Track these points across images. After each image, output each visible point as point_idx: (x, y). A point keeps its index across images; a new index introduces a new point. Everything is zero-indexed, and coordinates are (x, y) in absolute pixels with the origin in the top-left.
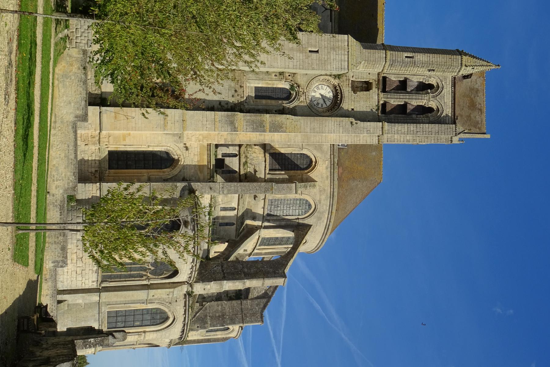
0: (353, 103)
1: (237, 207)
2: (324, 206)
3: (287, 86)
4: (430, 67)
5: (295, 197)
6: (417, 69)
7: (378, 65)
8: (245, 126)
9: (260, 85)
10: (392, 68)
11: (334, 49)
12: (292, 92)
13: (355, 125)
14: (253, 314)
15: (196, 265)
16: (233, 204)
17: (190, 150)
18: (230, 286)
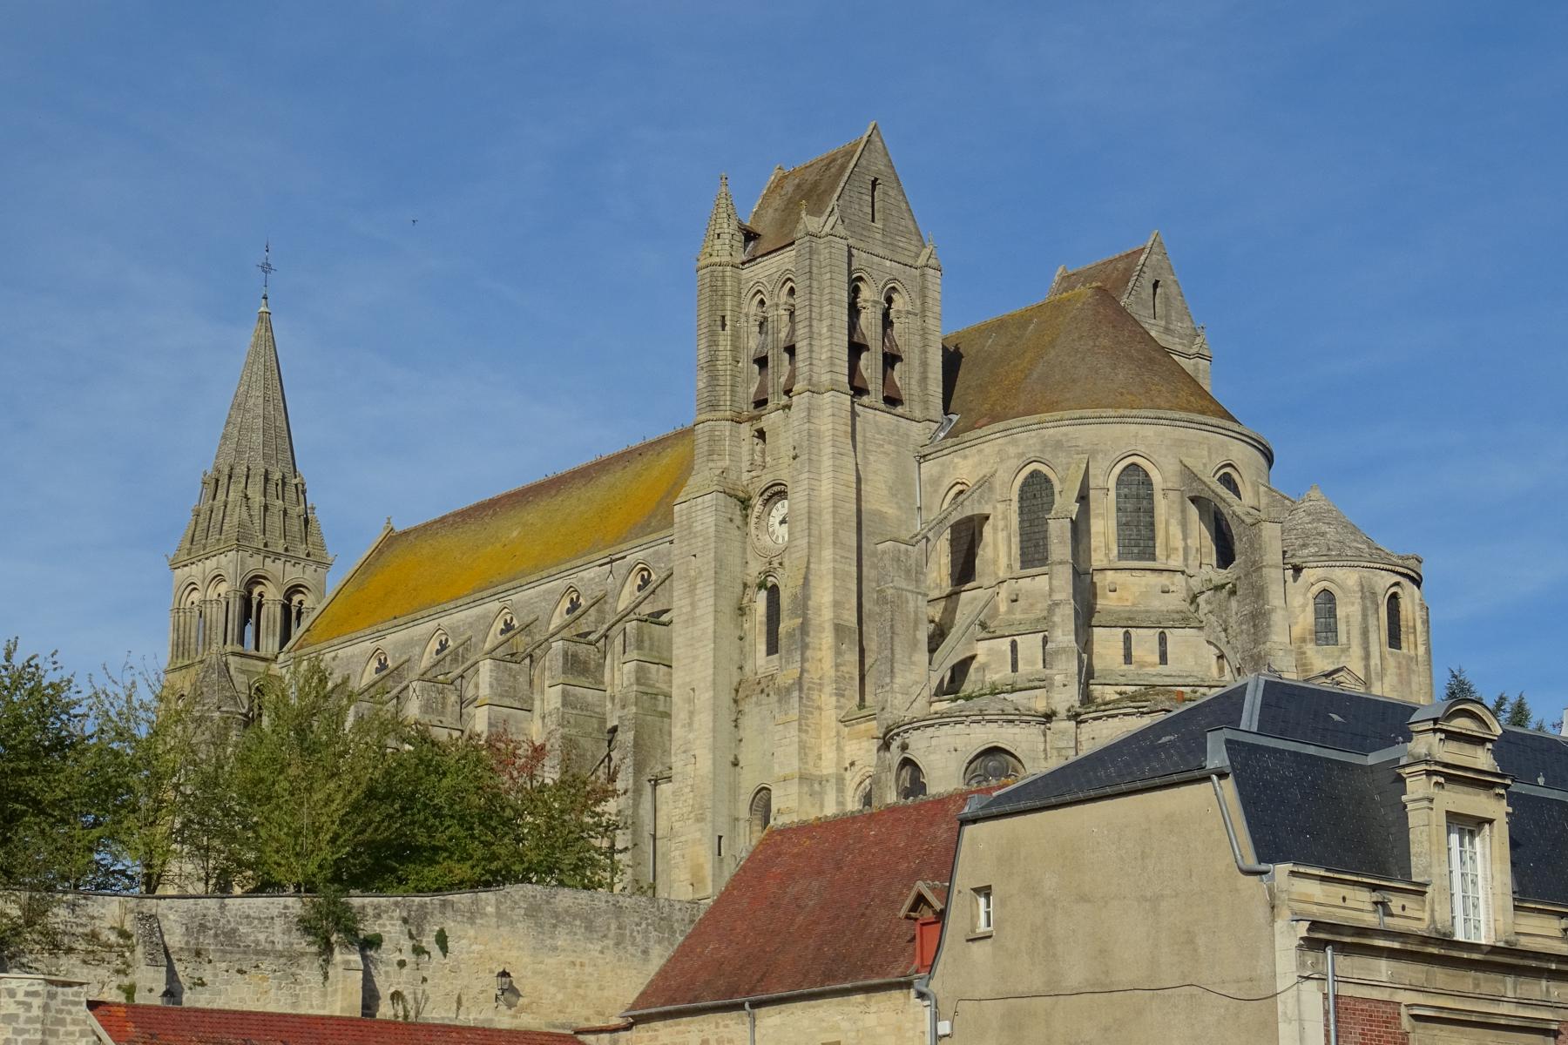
0: (781, 461)
1: (1010, 639)
2: (1031, 442)
3: (763, 594)
4: (714, 328)
5: (1015, 512)
6: (720, 353)
7: (717, 433)
8: (794, 666)
9: (762, 647)
10: (722, 403)
11: (690, 527)
12: (769, 585)
13: (797, 451)
14: (1252, 545)
15: (967, 716)
16: (1004, 648)
17: (856, 759)
18: (1063, 631)
